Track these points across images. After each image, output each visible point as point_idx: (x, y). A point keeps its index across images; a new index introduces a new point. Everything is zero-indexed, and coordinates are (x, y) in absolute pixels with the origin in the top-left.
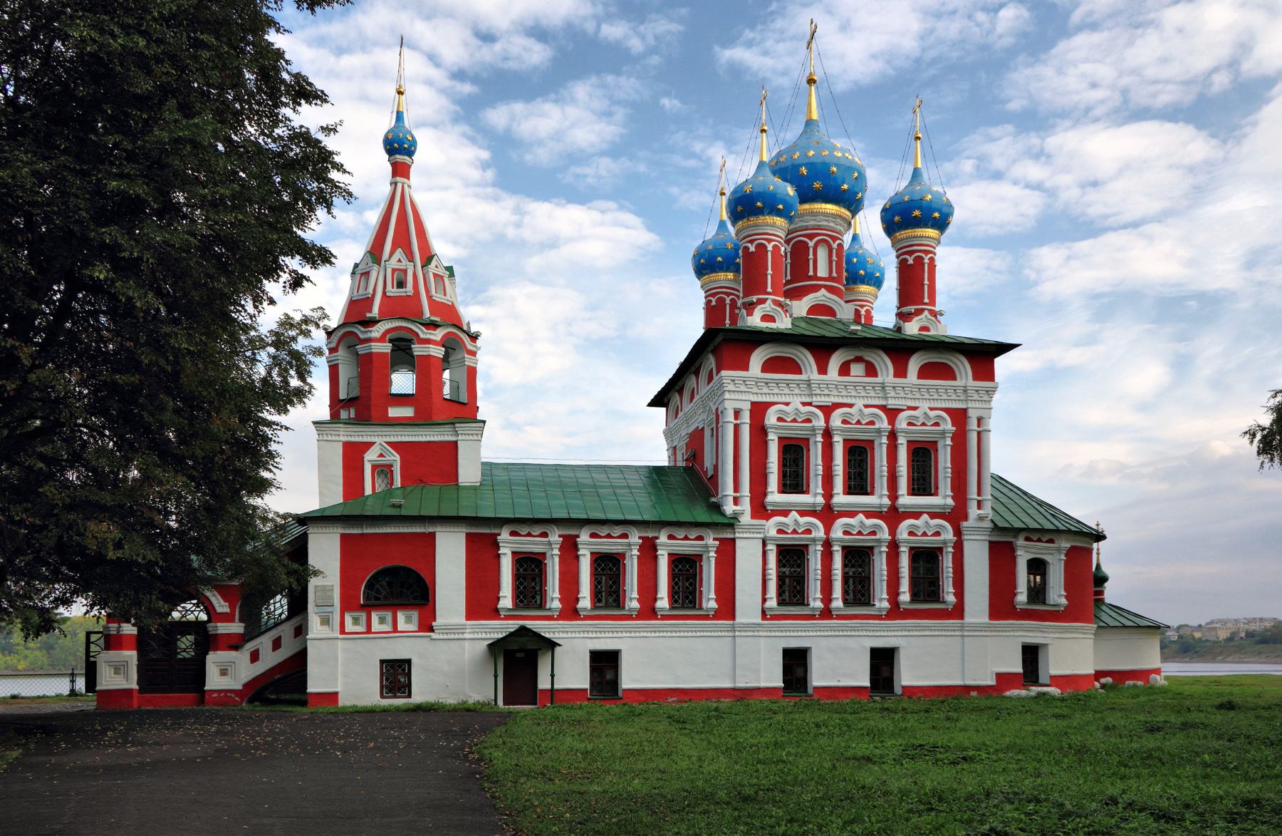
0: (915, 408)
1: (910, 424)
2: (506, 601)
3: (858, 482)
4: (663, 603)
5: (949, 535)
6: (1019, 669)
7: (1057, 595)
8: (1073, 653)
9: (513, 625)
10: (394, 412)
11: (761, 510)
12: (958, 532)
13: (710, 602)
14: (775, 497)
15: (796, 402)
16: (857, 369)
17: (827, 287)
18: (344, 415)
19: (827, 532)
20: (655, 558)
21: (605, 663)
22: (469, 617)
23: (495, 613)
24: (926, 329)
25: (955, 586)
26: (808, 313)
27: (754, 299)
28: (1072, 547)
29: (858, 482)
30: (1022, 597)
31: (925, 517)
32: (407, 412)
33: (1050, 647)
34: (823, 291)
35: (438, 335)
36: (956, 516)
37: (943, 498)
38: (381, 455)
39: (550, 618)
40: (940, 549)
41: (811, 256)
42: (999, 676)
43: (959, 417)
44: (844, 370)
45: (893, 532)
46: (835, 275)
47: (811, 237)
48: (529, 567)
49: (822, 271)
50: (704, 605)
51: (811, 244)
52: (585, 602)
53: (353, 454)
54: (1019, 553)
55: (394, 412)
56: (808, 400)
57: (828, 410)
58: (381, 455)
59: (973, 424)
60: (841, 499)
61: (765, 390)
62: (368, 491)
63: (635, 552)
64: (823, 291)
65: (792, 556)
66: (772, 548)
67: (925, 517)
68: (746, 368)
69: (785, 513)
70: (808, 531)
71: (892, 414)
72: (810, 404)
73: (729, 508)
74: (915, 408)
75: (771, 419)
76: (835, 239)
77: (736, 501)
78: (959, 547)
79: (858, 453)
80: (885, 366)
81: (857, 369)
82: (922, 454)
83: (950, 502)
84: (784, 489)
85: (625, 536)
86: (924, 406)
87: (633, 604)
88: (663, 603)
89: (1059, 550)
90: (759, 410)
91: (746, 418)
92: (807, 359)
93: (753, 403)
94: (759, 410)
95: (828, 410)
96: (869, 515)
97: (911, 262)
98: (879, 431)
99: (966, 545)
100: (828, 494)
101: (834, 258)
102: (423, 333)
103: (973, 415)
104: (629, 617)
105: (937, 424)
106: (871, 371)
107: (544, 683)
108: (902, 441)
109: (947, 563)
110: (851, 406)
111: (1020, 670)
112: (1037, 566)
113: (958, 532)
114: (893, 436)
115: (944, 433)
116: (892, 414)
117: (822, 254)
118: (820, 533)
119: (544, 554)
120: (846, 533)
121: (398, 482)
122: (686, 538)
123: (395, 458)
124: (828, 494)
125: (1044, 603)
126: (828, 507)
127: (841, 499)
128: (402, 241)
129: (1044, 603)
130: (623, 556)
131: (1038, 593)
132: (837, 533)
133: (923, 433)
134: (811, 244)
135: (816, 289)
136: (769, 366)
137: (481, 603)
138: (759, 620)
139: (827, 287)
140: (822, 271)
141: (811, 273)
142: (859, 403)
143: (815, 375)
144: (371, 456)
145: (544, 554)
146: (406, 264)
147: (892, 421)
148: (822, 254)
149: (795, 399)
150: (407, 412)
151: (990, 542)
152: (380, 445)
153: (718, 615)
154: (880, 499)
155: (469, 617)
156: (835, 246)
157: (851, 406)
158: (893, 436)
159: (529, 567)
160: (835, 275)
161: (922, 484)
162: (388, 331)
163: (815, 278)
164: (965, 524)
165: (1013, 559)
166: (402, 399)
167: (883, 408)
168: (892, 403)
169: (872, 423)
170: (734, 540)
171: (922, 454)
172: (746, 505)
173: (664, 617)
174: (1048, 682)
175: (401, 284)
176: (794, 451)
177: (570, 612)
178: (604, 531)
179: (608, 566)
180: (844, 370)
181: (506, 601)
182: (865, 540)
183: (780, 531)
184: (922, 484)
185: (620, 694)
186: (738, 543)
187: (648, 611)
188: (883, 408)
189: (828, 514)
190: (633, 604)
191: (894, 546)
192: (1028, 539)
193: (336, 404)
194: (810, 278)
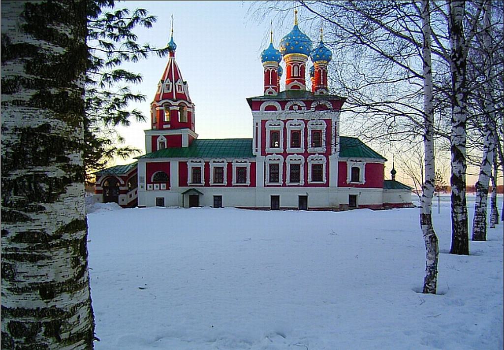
4: (234, 182)
10: (165, 127)
11: (263, 153)
12: (328, 159)
17: (297, 80)
18: (154, 128)
19: (285, 159)
22: (180, 186)
23: (187, 185)
25: (326, 176)
26: (291, 88)
28: (367, 163)
29: (296, 142)
32: (169, 126)
34: (296, 81)
35: (177, 103)
36: (327, 154)
37: (323, 149)
38: (162, 139)
39: (202, 186)
43: (329, 122)
46: (300, 75)
51: (292, 66)
52: (211, 182)
53: (154, 139)
55: (165, 127)
57: (285, 122)
58: (162, 139)
59: (333, 123)
62: (158, 149)
64: (296, 81)
65: (274, 168)
71: (306, 122)
72: (280, 120)
73: (254, 153)
75: (267, 124)
76: (300, 64)
77: (257, 151)
79: (295, 135)
84: (272, 146)
90: (264, 122)
91: (260, 124)
94: (264, 122)
95: (285, 122)
96: (298, 154)
102: (173, 103)
110: (293, 120)
111: (348, 203)
112: (356, 171)
121: (166, 147)
123: (165, 140)
125: (358, 181)
127: (289, 150)
128: (170, 76)
131: (355, 177)
135: (293, 80)
136: (268, 108)
137: (183, 182)
139: (297, 80)
141: (292, 76)
142: (295, 119)
144: (159, 140)
146: (170, 81)
147: (306, 125)
148: (296, 68)
149: (275, 119)
150: (169, 126)
152: (162, 136)
153: (250, 186)
154: (302, 150)
155: (180, 186)
156: (300, 66)
157: (293, 120)
161: (317, 142)
162: (163, 104)
164: (330, 157)
166: (167, 123)
167: (303, 120)
171: (316, 134)
172: (259, 151)
173: (235, 186)
175: (169, 89)
177: (207, 184)
180: (291, 108)
187: (229, 184)
188: (303, 120)
189: (285, 154)
191: (306, 164)
193: (153, 124)
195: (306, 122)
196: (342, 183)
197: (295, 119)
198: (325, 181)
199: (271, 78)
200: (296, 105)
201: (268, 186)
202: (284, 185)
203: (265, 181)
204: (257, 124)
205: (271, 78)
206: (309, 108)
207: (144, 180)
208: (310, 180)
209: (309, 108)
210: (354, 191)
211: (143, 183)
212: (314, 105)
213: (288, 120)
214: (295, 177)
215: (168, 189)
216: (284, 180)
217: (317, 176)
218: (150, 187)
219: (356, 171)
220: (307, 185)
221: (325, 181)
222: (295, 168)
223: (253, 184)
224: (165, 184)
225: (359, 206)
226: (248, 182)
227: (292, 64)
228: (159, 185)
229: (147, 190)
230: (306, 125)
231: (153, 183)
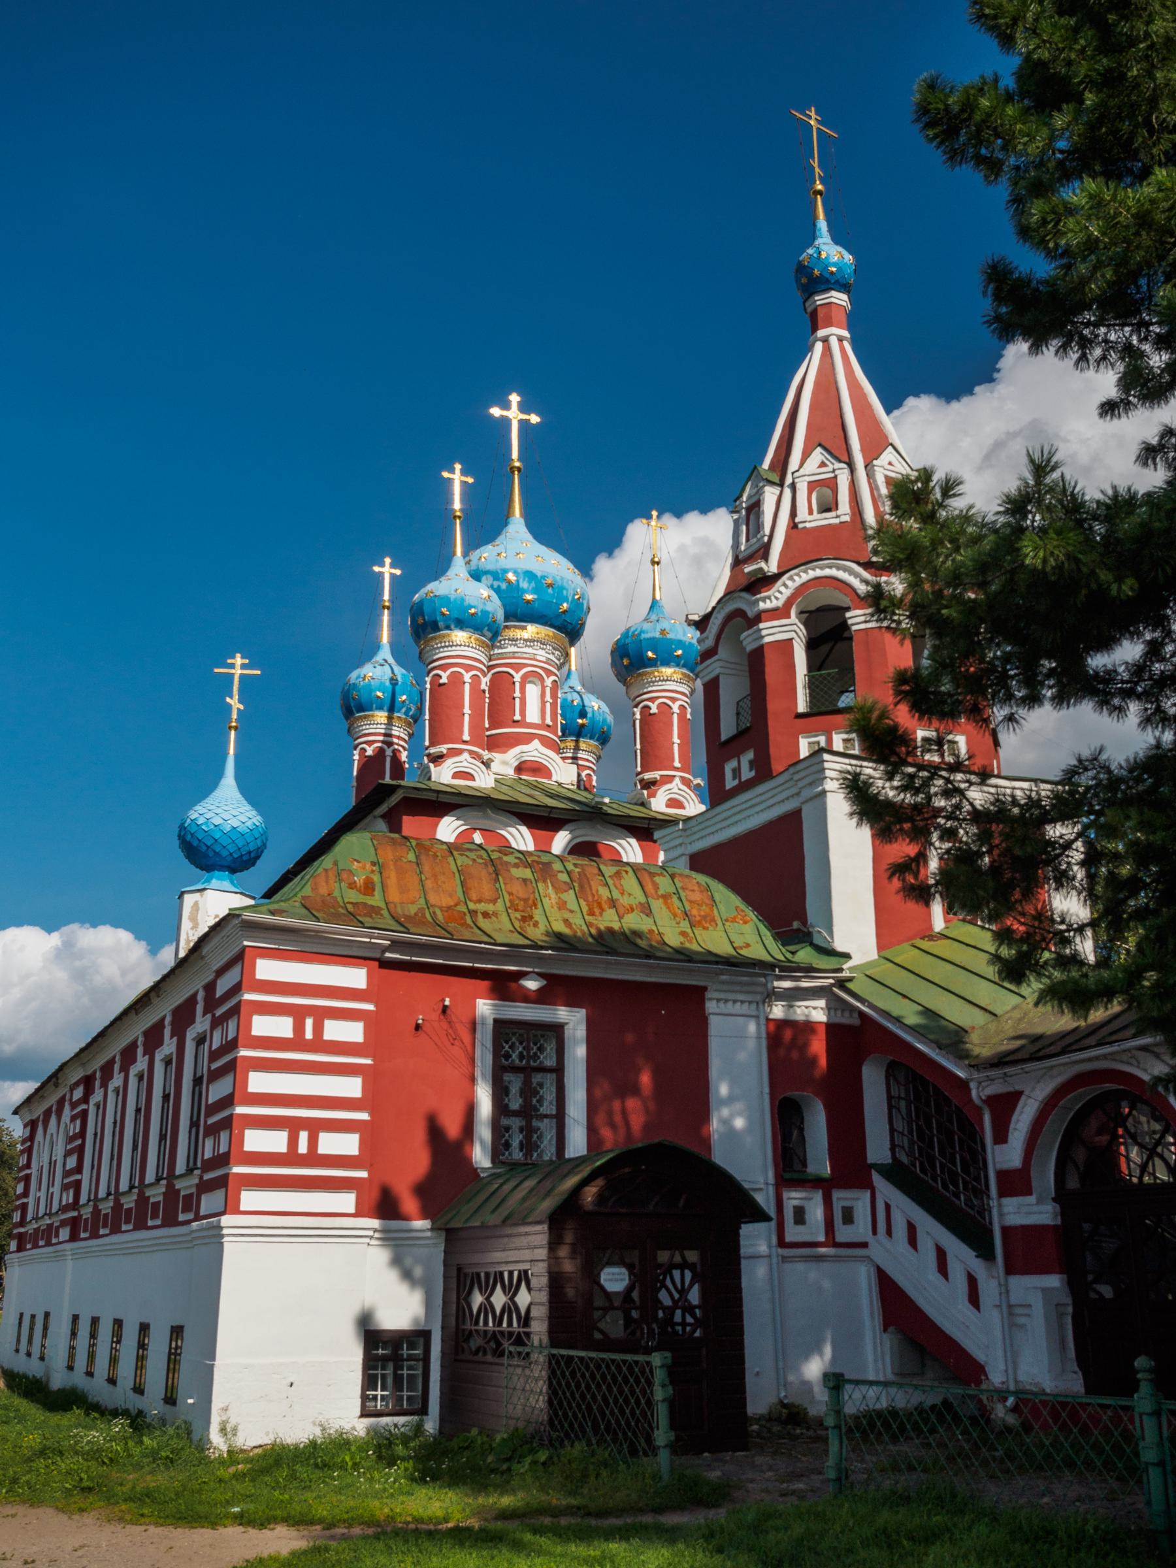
27: (443, 748)
41: (517, 694)
46: (548, 721)
47: (517, 667)
49: (533, 716)
76: (549, 673)
97: (654, 710)
101: (548, 698)
117: (533, 691)
134: (517, 677)
140: (533, 716)
141: (517, 717)
148: (533, 691)
156: (548, 682)
160: (548, 721)
163: (521, 723)
194: (516, 723)
199: (467, 710)
205: (467, 710)
227: (517, 667)
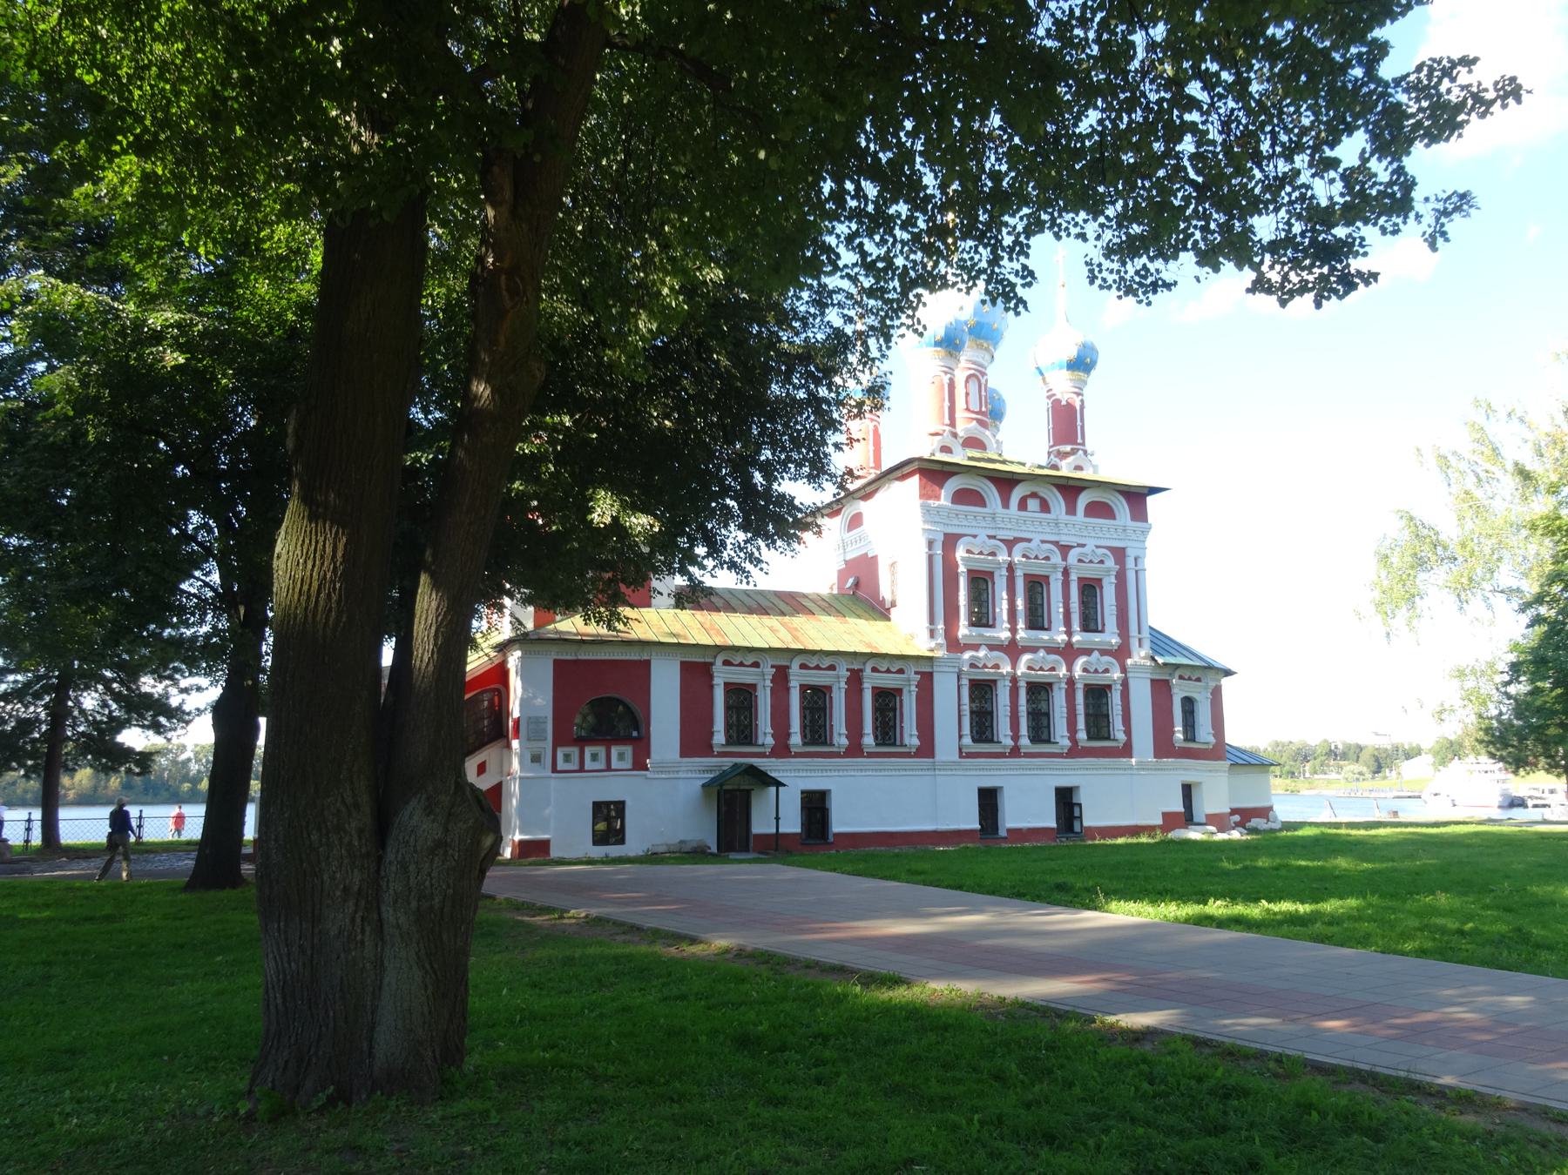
0: (1083, 546)
1: (1080, 561)
2: (719, 738)
3: (1037, 620)
4: (869, 740)
5: (1117, 675)
6: (1178, 807)
7: (1205, 734)
8: (1218, 792)
9: (728, 762)
11: (954, 644)
13: (911, 738)
14: (963, 630)
15: (983, 534)
16: (1033, 504)
20: (861, 690)
21: (816, 805)
22: (683, 754)
24: (1078, 468)
29: (1037, 620)
30: (1180, 736)
31: (1096, 654)
33: (1204, 787)
36: (1121, 653)
39: (762, 755)
40: (1109, 687)
42: (1165, 815)
43: (1119, 554)
44: (1023, 505)
45: (1070, 669)
48: (741, 698)
50: (907, 741)
52: (796, 739)
54: (1175, 690)
56: (992, 533)
57: (1010, 544)
59: (1130, 563)
60: (1022, 634)
61: (956, 522)
63: (843, 685)
65: (982, 690)
66: (965, 682)
67: (1096, 654)
68: (938, 498)
69: (976, 647)
70: (997, 666)
72: (993, 537)
74: (1083, 546)
75: (960, 553)
78: (1125, 683)
80: (1058, 502)
81: (1033, 504)
82: (1090, 589)
83: (1115, 640)
85: (832, 668)
86: (1091, 544)
87: (841, 740)
88: (869, 740)
89: (1206, 688)
90: (950, 541)
92: (991, 493)
93: (946, 535)
95: (1010, 544)
98: (1055, 567)
99: (1132, 683)
100: (1013, 630)
103: (1131, 554)
104: (837, 755)
105: (1102, 562)
106: (1045, 507)
107: (761, 824)
108: (1074, 577)
109: (1116, 698)
110: (1029, 540)
113: (1124, 670)
114: (1066, 572)
115: (1108, 570)
116: (1065, 550)
118: (1006, 669)
119: (754, 686)
120: (1030, 668)
122: (888, 671)
124: (1013, 630)
126: (1013, 641)
129: (1194, 740)
130: (829, 688)
132: (1022, 669)
133: (1090, 572)
137: (695, 741)
138: (956, 757)
142: (1037, 538)
143: (999, 509)
145: (754, 686)
147: (1065, 558)
151: (1153, 681)
157: (1029, 540)
158: (1066, 572)
159: (741, 698)
164: (1129, 661)
165: (1171, 696)
167: (1056, 543)
168: (1064, 540)
169: (1047, 558)
170: (931, 674)
172: (941, 640)
173: (871, 755)
174: (1204, 820)
176: (980, 582)
177: (782, 749)
178: (813, 662)
179: (816, 699)
180: (1023, 505)
181: (719, 738)
182: (1042, 676)
183: (973, 666)
184: (1090, 623)
185: (831, 839)
186: (936, 677)
187: (855, 750)
190: (841, 740)
192: (1181, 677)
195: (1065, 550)
196: (1164, 747)
197: (1037, 538)
198: (1121, 736)
200: (1034, 495)
201: (970, 755)
202: (1015, 752)
203: (960, 737)
204: (930, 544)
206: (1071, 510)
207: (545, 731)
208: (1082, 735)
209: (1071, 510)
210: (1191, 771)
211: (541, 744)
212: (1083, 500)
213: (1017, 540)
214: (1040, 728)
215: (639, 765)
216: (1016, 737)
217: (1098, 723)
218: (567, 758)
219: (1188, 703)
220: (1075, 752)
221: (1121, 736)
222: (1039, 690)
223: (927, 748)
224: (628, 750)
225: (1208, 816)
226: (911, 738)
228: (601, 750)
229: (554, 770)
230: (1065, 558)
231: (581, 742)
